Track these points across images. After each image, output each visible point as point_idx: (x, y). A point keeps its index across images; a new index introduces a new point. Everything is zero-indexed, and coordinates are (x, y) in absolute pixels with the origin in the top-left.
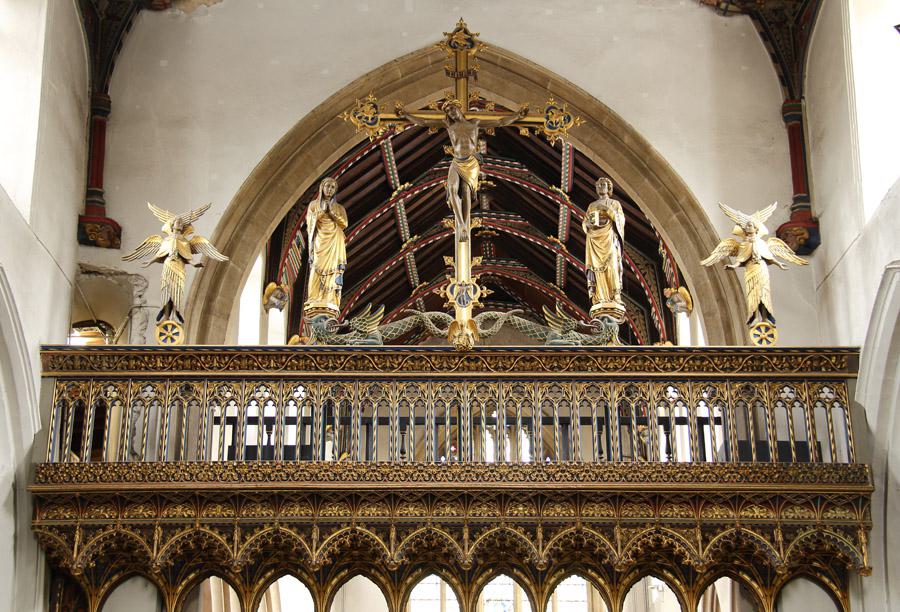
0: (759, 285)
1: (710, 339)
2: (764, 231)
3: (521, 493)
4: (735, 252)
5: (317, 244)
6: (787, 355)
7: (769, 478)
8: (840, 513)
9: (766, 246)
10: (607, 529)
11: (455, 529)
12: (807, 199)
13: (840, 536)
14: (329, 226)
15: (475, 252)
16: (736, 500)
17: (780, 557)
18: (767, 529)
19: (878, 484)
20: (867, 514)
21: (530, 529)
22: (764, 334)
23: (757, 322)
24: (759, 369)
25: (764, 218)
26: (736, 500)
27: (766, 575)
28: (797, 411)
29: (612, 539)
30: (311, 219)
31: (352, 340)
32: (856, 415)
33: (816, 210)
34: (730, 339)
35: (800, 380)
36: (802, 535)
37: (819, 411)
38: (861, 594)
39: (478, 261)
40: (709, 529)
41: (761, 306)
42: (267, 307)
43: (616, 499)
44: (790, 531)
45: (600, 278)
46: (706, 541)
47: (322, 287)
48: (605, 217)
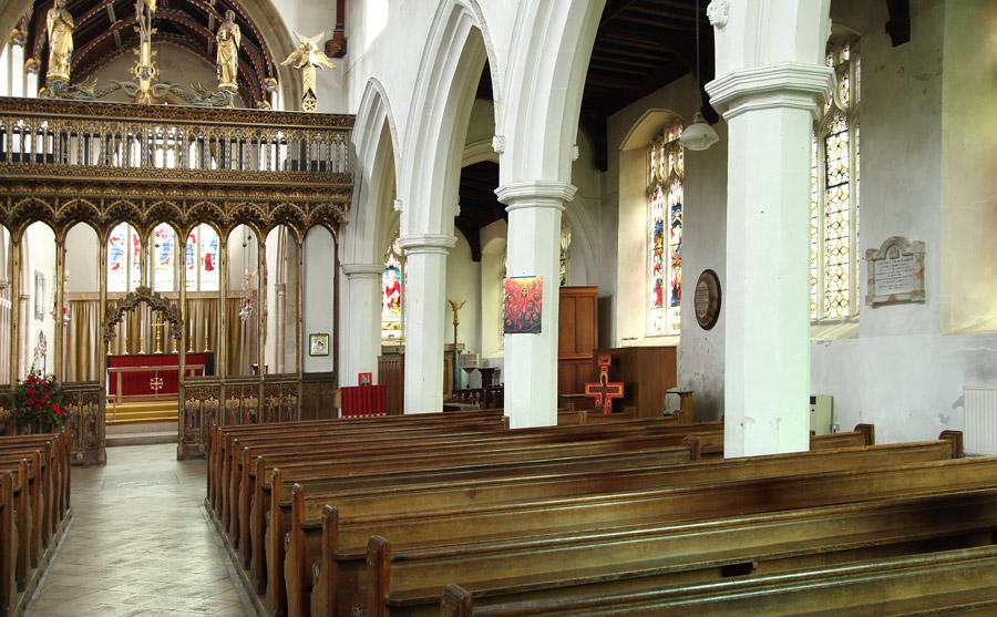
0: (310, 79)
1: (286, 105)
2: (315, 48)
3: (175, 184)
4: (299, 59)
5: (54, 37)
6: (320, 117)
7: (305, 180)
8: (337, 196)
9: (317, 57)
10: (221, 203)
11: (138, 202)
12: (343, 27)
13: (336, 207)
14: (63, 27)
15: (152, 48)
16: (288, 190)
17: (306, 218)
18: (302, 204)
19: (357, 182)
20: (350, 197)
21: (179, 203)
22: (310, 105)
23: (307, 99)
24: (306, 124)
25: (316, 42)
26: (288, 190)
27: (301, 225)
28: (323, 144)
29: (223, 208)
30: (50, 22)
31: (78, 97)
32: (351, 148)
33: (346, 36)
34: (296, 107)
35: (326, 130)
36: (319, 207)
37: (334, 145)
38: (344, 233)
39: (154, 53)
40: (273, 204)
41: (310, 90)
42: (26, 72)
43: (226, 188)
44: (313, 205)
45: (224, 68)
46: (271, 209)
47: (58, 64)
48: (229, 35)
